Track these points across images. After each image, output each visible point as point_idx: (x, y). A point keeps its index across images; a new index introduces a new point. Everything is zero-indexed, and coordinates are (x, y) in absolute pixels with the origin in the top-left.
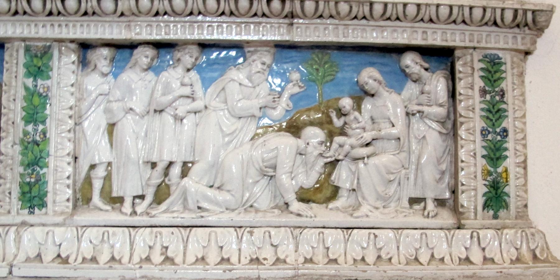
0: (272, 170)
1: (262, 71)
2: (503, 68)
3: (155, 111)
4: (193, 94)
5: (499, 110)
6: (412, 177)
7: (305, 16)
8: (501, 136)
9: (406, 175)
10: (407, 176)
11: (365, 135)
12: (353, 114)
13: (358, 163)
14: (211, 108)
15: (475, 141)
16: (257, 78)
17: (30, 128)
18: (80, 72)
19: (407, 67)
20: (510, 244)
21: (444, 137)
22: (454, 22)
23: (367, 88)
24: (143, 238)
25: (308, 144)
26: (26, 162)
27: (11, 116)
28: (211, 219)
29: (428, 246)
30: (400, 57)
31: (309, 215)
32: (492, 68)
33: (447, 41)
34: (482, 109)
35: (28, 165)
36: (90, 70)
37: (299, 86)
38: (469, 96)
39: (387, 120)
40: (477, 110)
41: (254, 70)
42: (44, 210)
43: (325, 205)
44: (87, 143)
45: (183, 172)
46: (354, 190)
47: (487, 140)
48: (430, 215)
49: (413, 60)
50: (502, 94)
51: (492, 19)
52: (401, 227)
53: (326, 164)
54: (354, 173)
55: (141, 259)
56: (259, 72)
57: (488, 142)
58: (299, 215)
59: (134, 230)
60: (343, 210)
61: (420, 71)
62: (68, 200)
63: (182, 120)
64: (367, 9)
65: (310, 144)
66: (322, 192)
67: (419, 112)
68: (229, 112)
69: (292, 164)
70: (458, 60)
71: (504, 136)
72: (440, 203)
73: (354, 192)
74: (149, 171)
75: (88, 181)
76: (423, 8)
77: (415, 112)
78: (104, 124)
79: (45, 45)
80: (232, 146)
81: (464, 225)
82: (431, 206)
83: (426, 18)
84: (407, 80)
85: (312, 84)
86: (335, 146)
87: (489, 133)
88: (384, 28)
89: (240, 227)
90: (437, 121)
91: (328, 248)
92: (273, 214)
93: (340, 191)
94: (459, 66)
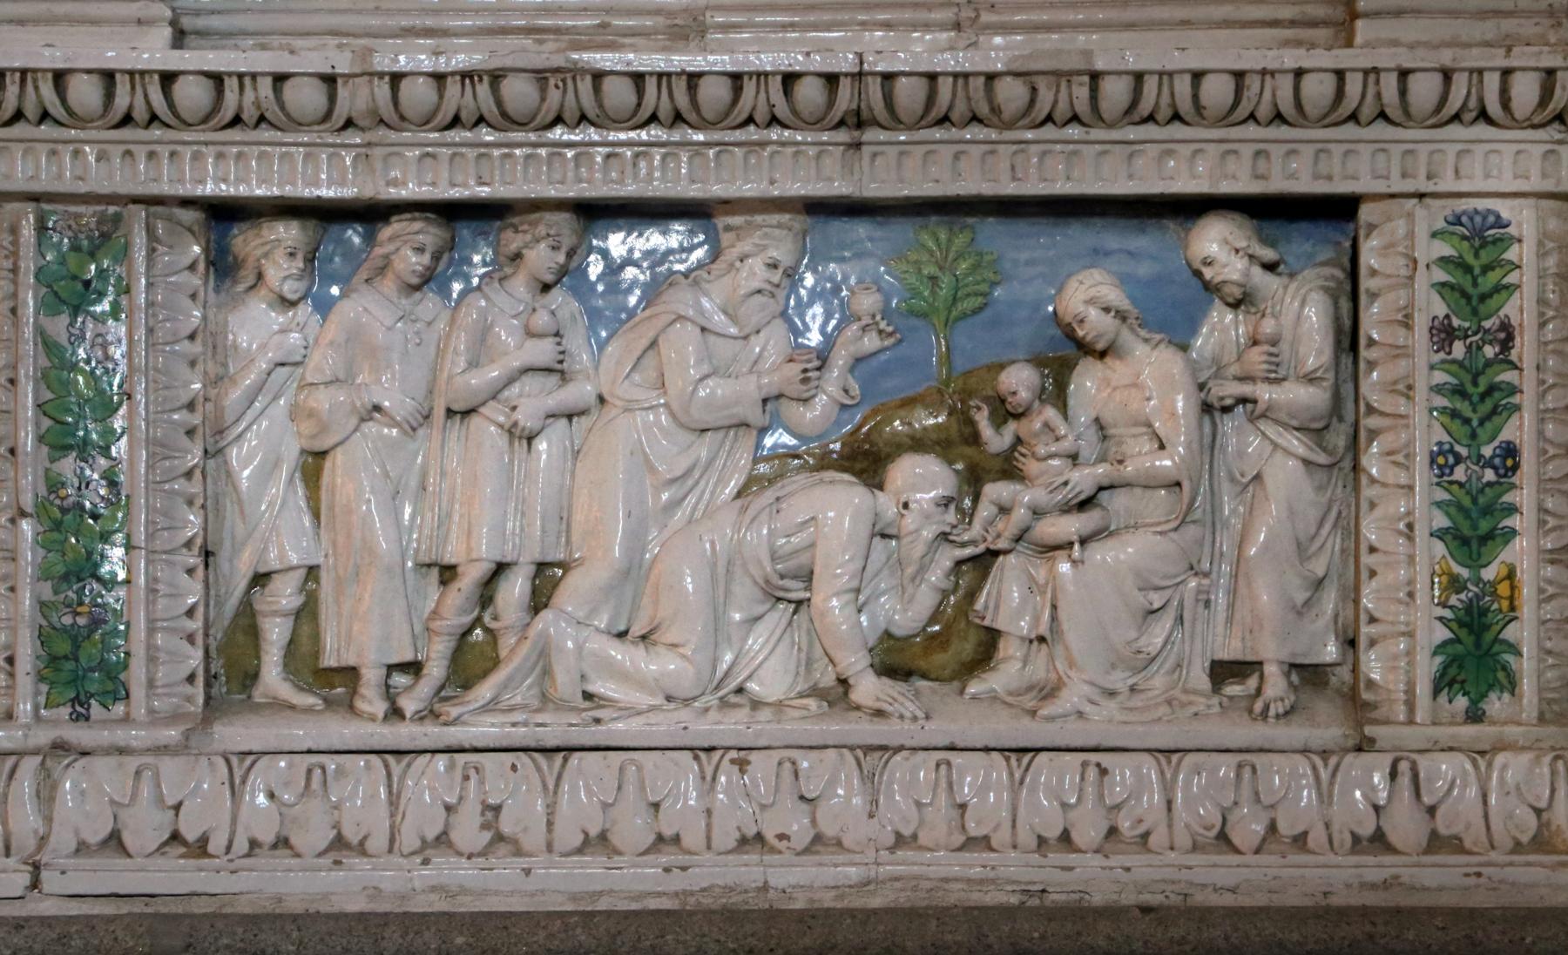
0: (802, 585)
1: (768, 287)
2: (1511, 254)
3: (450, 413)
4: (561, 362)
5: (1492, 389)
6: (1221, 599)
7: (895, 121)
8: (1495, 468)
9: (1199, 592)
10: (1204, 597)
12: (1040, 412)
13: (1053, 559)
14: (618, 403)
15: (1411, 488)
17: (68, 466)
18: (212, 295)
19: (1208, 262)
20: (1513, 799)
21: (1321, 476)
22: (1354, 117)
23: (1080, 333)
24: (428, 784)
25: (906, 506)
26: (60, 569)
28: (619, 729)
29: (1258, 800)
30: (1188, 231)
31: (908, 714)
32: (1476, 255)
33: (1330, 178)
34: (1438, 389)
35: (65, 577)
36: (240, 288)
37: (881, 332)
38: (1398, 347)
39: (1144, 430)
40: (1421, 392)
42: (119, 709)
43: (956, 684)
44: (242, 512)
46: (1042, 639)
47: (1451, 483)
48: (1272, 712)
50: (1506, 336)
51: (1473, 103)
52: (1181, 745)
53: (959, 563)
55: (424, 841)
56: (759, 292)
57: (1455, 488)
58: (879, 713)
59: (398, 762)
60: (1009, 699)
61: (1247, 274)
62: (191, 679)
63: (530, 439)
64: (1082, 92)
67: (1244, 401)
68: (672, 414)
69: (859, 564)
70: (1368, 236)
71: (1507, 469)
72: (1309, 675)
73: (1044, 646)
74: (434, 592)
75: (247, 624)
76: (1253, 83)
77: (1228, 402)
78: (291, 452)
79: (103, 213)
80: (680, 515)
81: (1372, 741)
82: (1276, 685)
83: (1264, 112)
86: (985, 511)
87: (1459, 459)
88: (1137, 147)
89: (710, 750)
90: (1297, 429)
91: (963, 807)
93: (1002, 644)
94: (1369, 257)
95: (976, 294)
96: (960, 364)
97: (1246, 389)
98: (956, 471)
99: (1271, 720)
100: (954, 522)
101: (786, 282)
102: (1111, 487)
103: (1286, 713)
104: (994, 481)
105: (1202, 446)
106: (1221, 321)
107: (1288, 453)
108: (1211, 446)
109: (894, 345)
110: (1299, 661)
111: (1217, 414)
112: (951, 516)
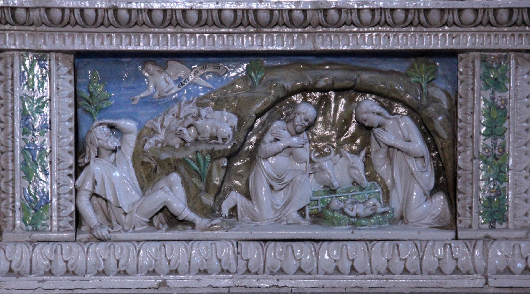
27: (469, 129)
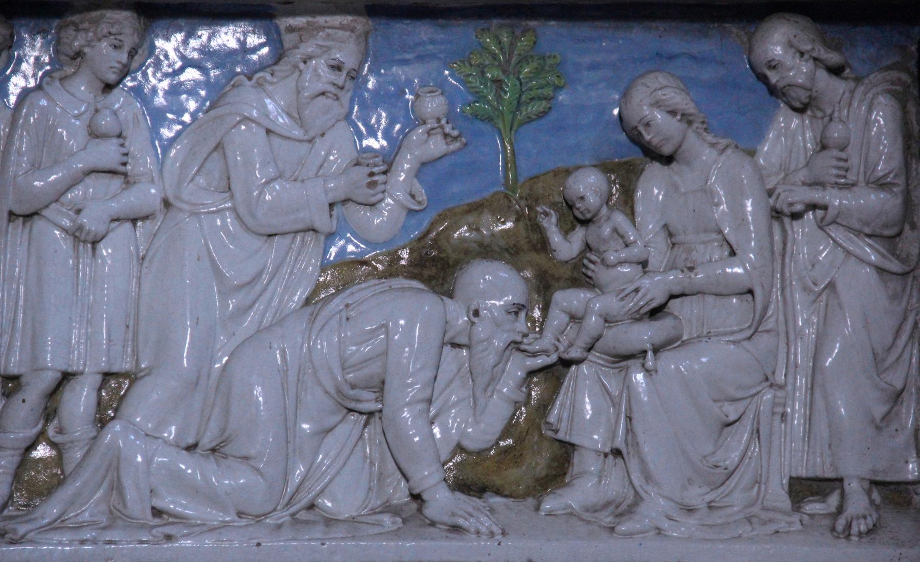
0: (372, 396)
1: (332, 89)
3: (12, 215)
4: (124, 164)
6: (797, 411)
9: (774, 404)
10: (779, 410)
11: (646, 282)
12: (609, 218)
16: (320, 112)
19: (773, 65)
21: (895, 284)
23: (648, 137)
25: (476, 313)
31: (483, 529)
37: (446, 135)
39: (714, 236)
41: (311, 85)
43: (531, 501)
45: (100, 405)
46: (617, 453)
48: (855, 530)
49: (790, 45)
53: (531, 373)
54: (616, 404)
56: (323, 94)
58: (456, 529)
60: (586, 516)
61: (812, 78)
63: (94, 243)
65: (483, 313)
66: (524, 464)
67: (813, 207)
68: (239, 217)
69: (430, 374)
73: (619, 461)
77: (798, 208)
80: (249, 322)
82: (858, 502)
84: (777, 106)
85: (485, 127)
86: (557, 318)
90: (869, 236)
92: (376, 530)
93: (576, 459)
95: (540, 98)
96: (526, 168)
97: (816, 195)
98: (526, 279)
99: (855, 539)
100: (525, 331)
101: (349, 85)
102: (683, 295)
103: (869, 532)
104: (563, 288)
105: (773, 252)
106: (787, 127)
107: (862, 261)
108: (779, 255)
109: (460, 149)
110: (880, 478)
111: (787, 220)
112: (522, 324)
